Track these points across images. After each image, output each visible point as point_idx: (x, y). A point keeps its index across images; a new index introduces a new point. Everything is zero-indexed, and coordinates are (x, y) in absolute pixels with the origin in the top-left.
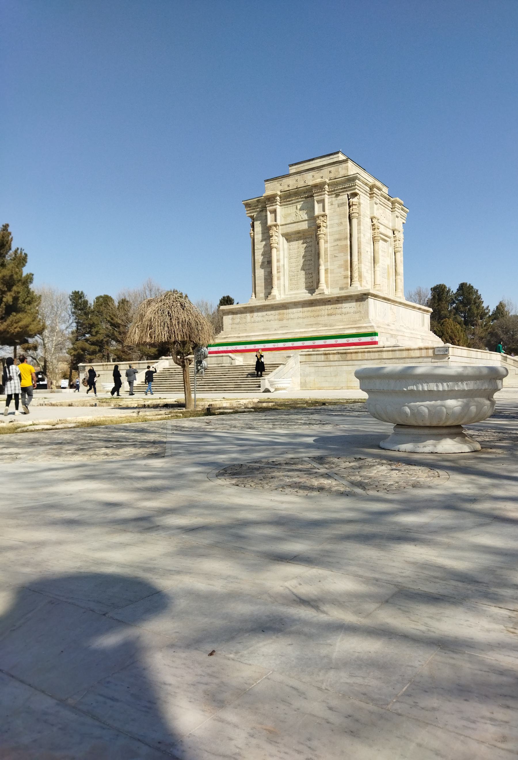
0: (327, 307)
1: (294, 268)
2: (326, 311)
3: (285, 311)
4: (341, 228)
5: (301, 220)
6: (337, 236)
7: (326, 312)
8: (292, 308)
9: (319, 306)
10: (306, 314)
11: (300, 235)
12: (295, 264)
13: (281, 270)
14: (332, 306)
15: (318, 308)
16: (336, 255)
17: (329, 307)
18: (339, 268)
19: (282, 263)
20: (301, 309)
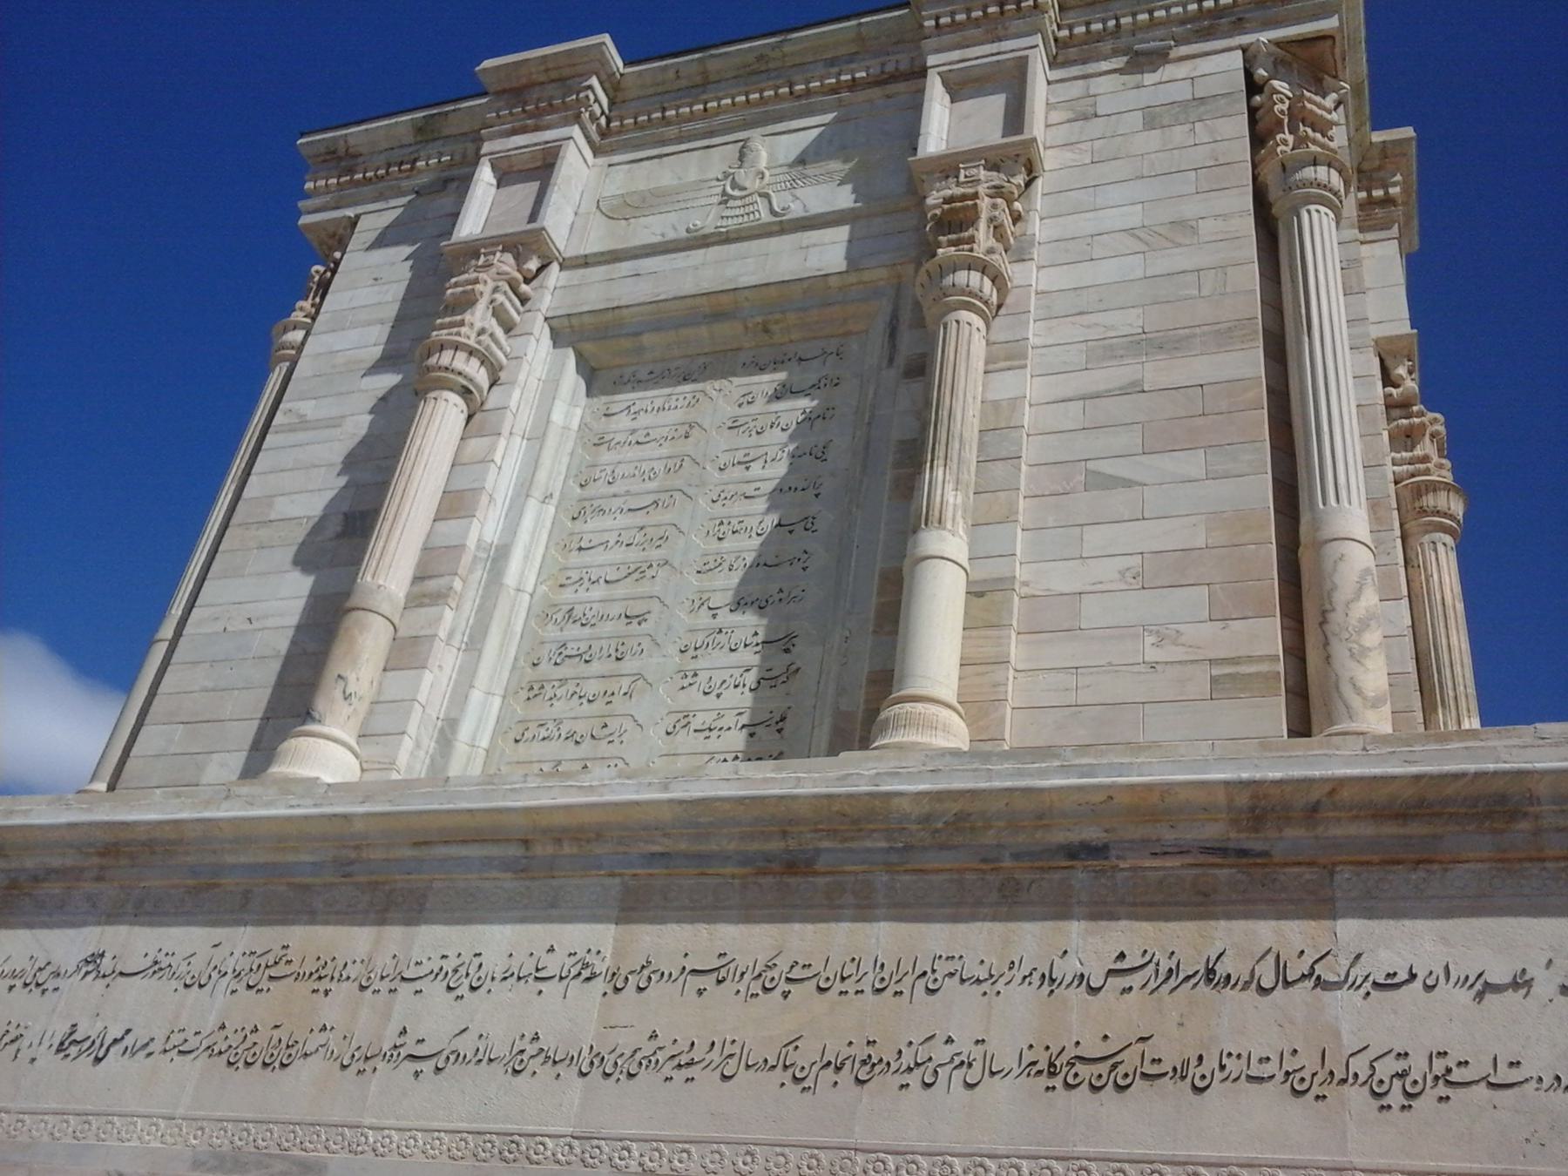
0: (1031, 939)
1: (598, 592)
2: (1020, 1002)
3: (355, 942)
4: (1181, 259)
5: (765, 217)
6: (1128, 321)
7: (1015, 1023)
8: (468, 908)
9: (911, 908)
10: (672, 1014)
11: (725, 329)
12: (618, 554)
13: (467, 586)
14: (1132, 936)
15: (883, 939)
16: (1106, 467)
17: (1087, 944)
18: (1143, 582)
19: (485, 527)
20: (597, 938)
